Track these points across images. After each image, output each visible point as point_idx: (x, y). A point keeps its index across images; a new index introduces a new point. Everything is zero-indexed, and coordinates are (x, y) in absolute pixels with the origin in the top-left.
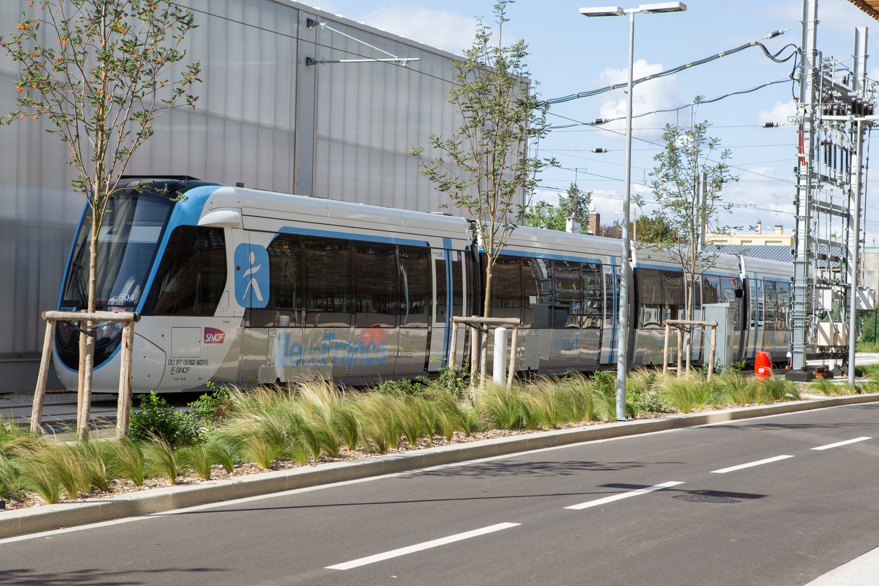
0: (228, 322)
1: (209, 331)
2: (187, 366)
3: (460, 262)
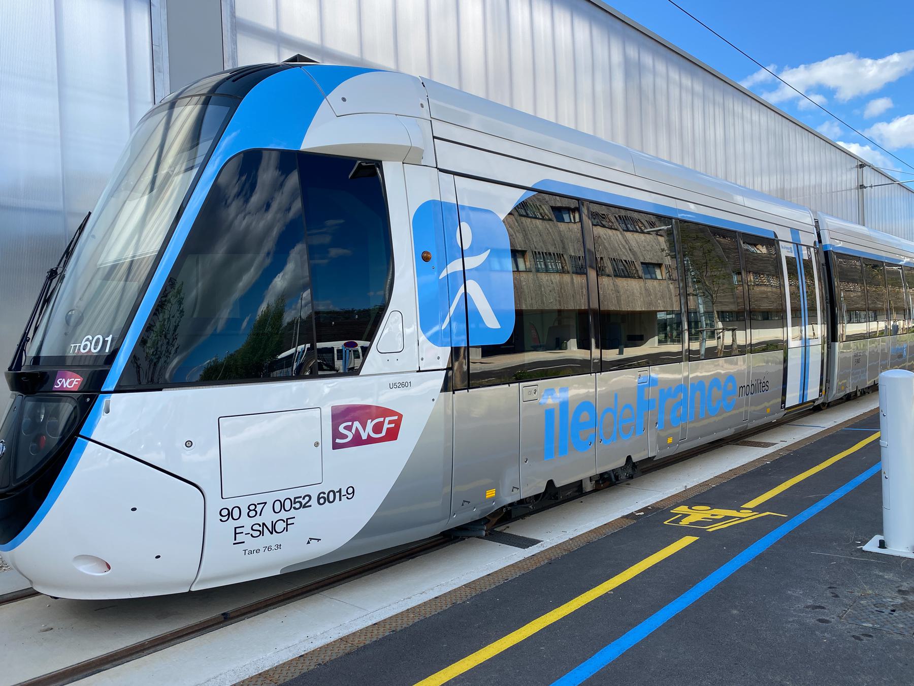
0: (404, 385)
1: (342, 415)
2: (284, 515)
3: (810, 260)
